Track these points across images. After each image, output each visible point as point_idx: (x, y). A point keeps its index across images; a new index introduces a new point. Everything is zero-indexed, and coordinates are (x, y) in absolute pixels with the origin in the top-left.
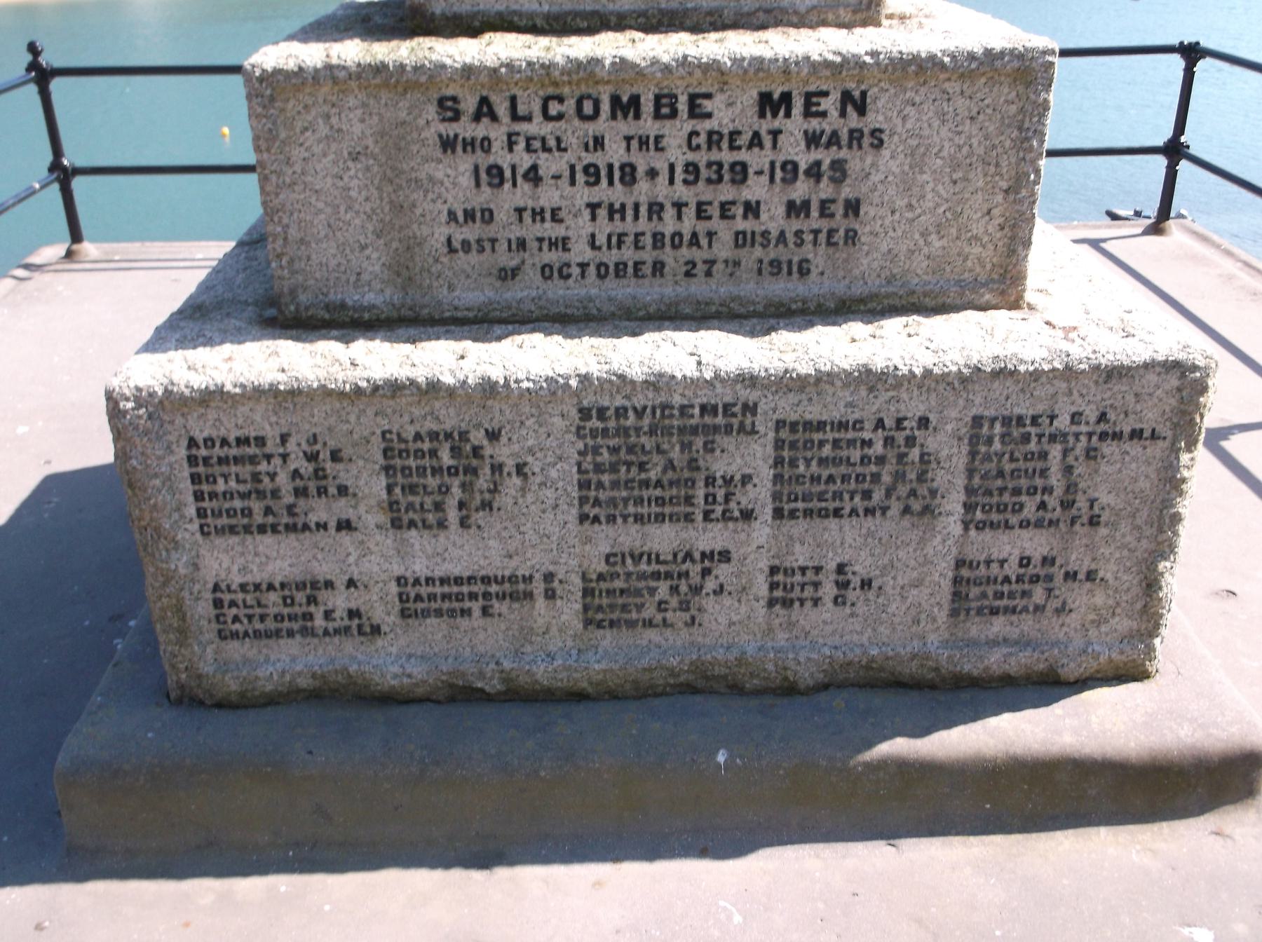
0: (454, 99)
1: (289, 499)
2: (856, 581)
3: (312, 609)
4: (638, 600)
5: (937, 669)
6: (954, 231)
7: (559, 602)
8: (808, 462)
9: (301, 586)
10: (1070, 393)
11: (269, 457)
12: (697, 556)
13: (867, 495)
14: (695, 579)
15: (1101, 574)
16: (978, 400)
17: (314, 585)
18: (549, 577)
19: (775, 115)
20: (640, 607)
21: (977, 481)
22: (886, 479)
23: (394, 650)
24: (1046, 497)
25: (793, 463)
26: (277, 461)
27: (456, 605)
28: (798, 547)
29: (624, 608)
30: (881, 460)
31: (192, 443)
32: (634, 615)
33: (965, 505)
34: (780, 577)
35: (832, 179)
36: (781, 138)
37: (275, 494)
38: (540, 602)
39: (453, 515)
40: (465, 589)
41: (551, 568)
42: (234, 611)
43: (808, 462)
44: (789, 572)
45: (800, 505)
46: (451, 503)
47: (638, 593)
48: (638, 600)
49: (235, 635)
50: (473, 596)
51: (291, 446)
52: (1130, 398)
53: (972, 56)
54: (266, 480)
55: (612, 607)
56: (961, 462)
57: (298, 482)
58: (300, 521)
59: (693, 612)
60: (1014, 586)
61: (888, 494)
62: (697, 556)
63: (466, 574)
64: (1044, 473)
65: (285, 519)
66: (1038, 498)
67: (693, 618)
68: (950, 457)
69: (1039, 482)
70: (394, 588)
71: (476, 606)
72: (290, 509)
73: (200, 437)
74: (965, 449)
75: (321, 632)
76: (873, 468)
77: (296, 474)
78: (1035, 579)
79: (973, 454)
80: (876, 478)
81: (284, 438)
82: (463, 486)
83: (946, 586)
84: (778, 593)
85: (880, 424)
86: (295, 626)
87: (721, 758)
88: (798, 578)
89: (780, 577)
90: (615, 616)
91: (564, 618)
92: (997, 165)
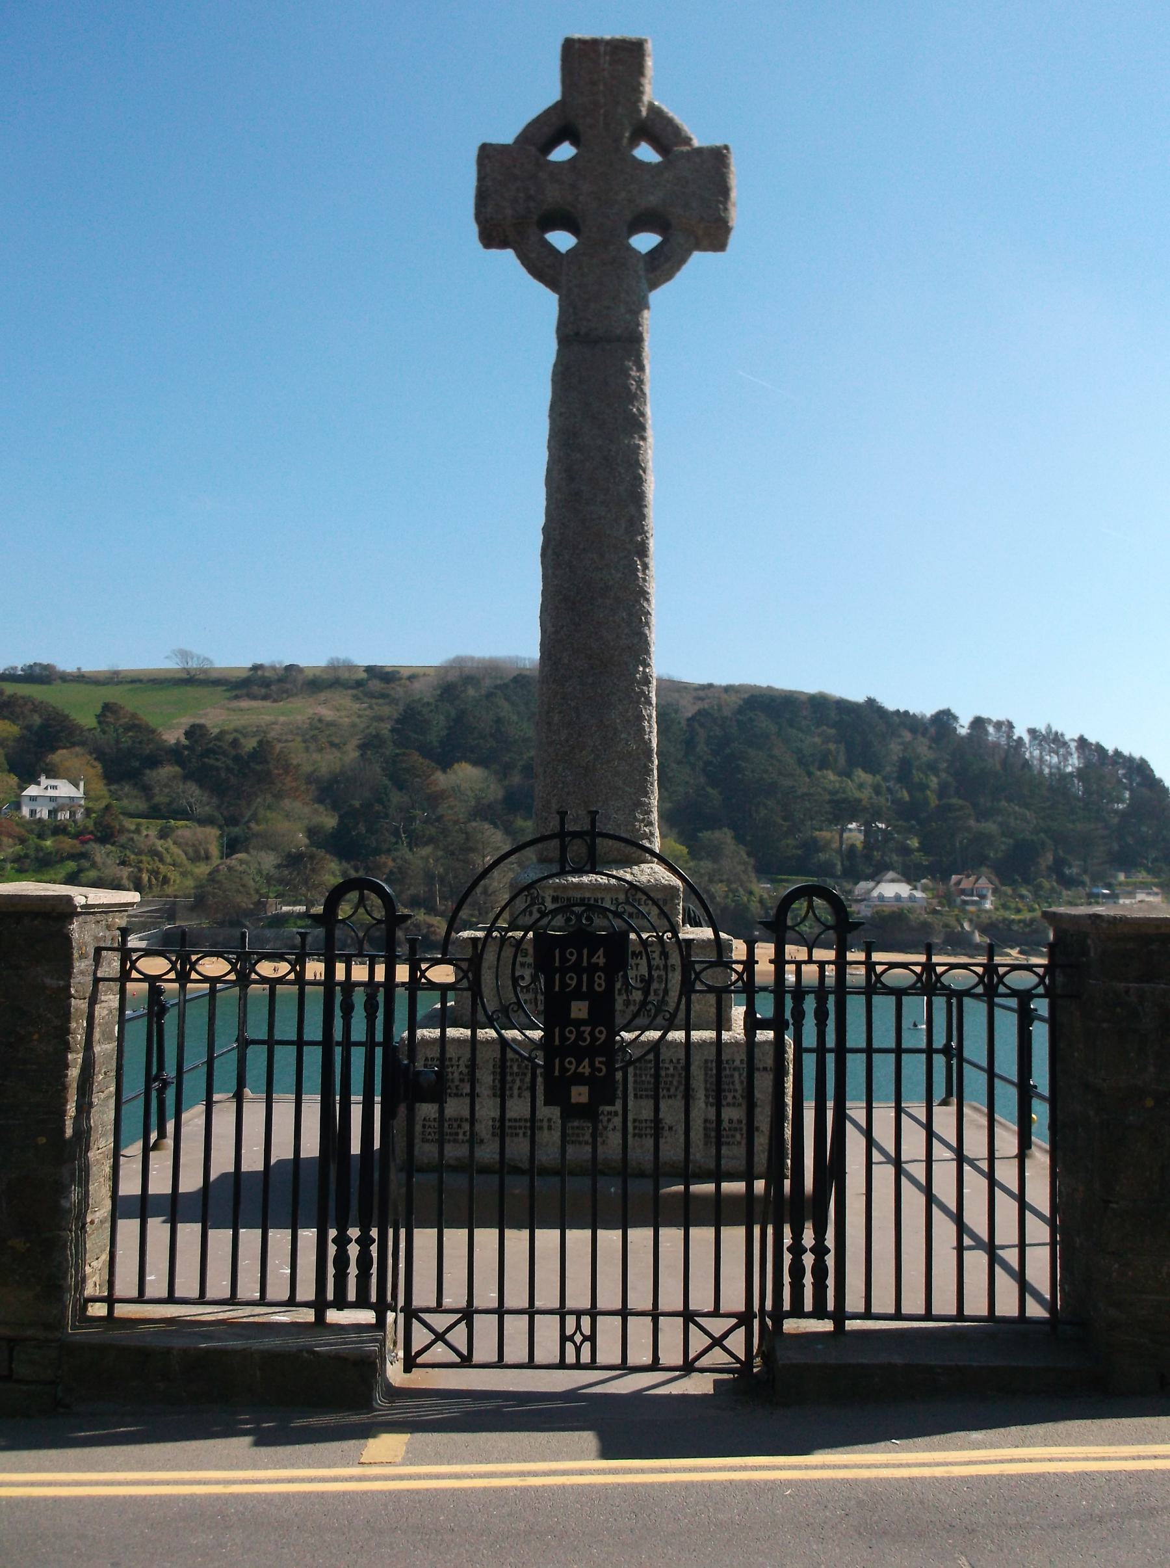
0: (526, 949)
1: (457, 1083)
2: (667, 1128)
3: (459, 1131)
4: (583, 1132)
5: (700, 1167)
6: (703, 1002)
7: (553, 1132)
8: (646, 1075)
9: (456, 1120)
10: (738, 1052)
11: (452, 1066)
12: (606, 1113)
13: (668, 1090)
14: (605, 1124)
15: (761, 1128)
16: (706, 1053)
17: (461, 1120)
18: (549, 1120)
19: (637, 958)
20: (583, 1135)
21: (708, 1086)
22: (675, 1083)
23: (488, 1150)
24: (735, 1094)
25: (641, 1076)
26: (455, 1068)
27: (514, 1131)
28: (644, 1111)
29: (578, 1135)
30: (673, 1076)
31: (427, 1059)
32: (581, 1139)
33: (705, 1095)
34: (637, 1124)
35: (658, 982)
36: (639, 967)
37: (453, 1081)
38: (546, 1131)
39: (516, 1092)
40: (517, 1124)
41: (551, 1116)
42: (430, 1130)
43: (646, 1075)
44: (641, 1121)
45: (644, 1093)
46: (516, 1087)
47: (583, 1129)
48: (583, 1132)
49: (428, 1141)
50: (520, 1127)
51: (461, 1062)
52: (761, 1054)
53: (703, 941)
54: (450, 1075)
55: (573, 1134)
56: (701, 1077)
57: (461, 1076)
58: (460, 1093)
59: (604, 1138)
60: (728, 1133)
61: (676, 1089)
62: (606, 1113)
63: (518, 1117)
64: (733, 1083)
65: (455, 1091)
66: (732, 1094)
67: (604, 1141)
68: (698, 1075)
69: (731, 1087)
70: (490, 1123)
71: (521, 1132)
72: (457, 1087)
73: (430, 1057)
74: (703, 1072)
75: (460, 1141)
76: (670, 1079)
77: (461, 1073)
78: (736, 1129)
79: (706, 1074)
80: (671, 1083)
81: (459, 1059)
82: (520, 1080)
83: (701, 1129)
84: (637, 1131)
85: (671, 1061)
86: (451, 1138)
87: (613, 1190)
88: (644, 1125)
89: (637, 1124)
90: (574, 1139)
91: (555, 1138)
92: (717, 979)
